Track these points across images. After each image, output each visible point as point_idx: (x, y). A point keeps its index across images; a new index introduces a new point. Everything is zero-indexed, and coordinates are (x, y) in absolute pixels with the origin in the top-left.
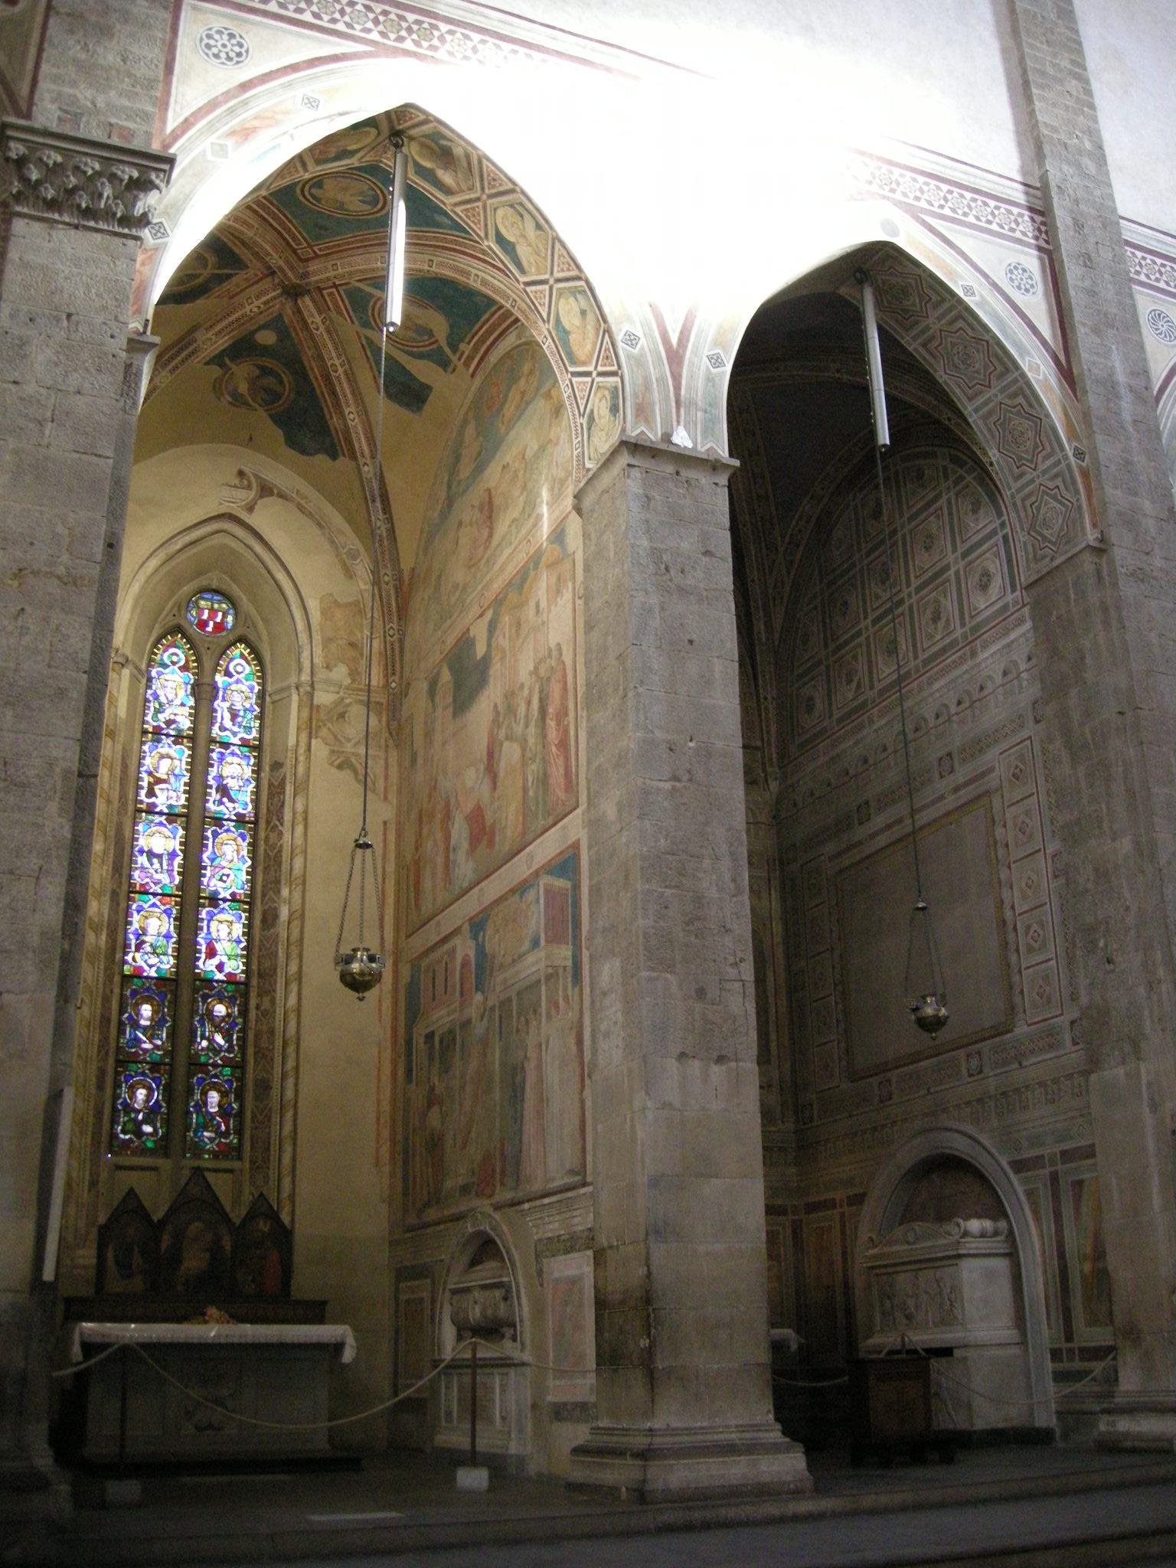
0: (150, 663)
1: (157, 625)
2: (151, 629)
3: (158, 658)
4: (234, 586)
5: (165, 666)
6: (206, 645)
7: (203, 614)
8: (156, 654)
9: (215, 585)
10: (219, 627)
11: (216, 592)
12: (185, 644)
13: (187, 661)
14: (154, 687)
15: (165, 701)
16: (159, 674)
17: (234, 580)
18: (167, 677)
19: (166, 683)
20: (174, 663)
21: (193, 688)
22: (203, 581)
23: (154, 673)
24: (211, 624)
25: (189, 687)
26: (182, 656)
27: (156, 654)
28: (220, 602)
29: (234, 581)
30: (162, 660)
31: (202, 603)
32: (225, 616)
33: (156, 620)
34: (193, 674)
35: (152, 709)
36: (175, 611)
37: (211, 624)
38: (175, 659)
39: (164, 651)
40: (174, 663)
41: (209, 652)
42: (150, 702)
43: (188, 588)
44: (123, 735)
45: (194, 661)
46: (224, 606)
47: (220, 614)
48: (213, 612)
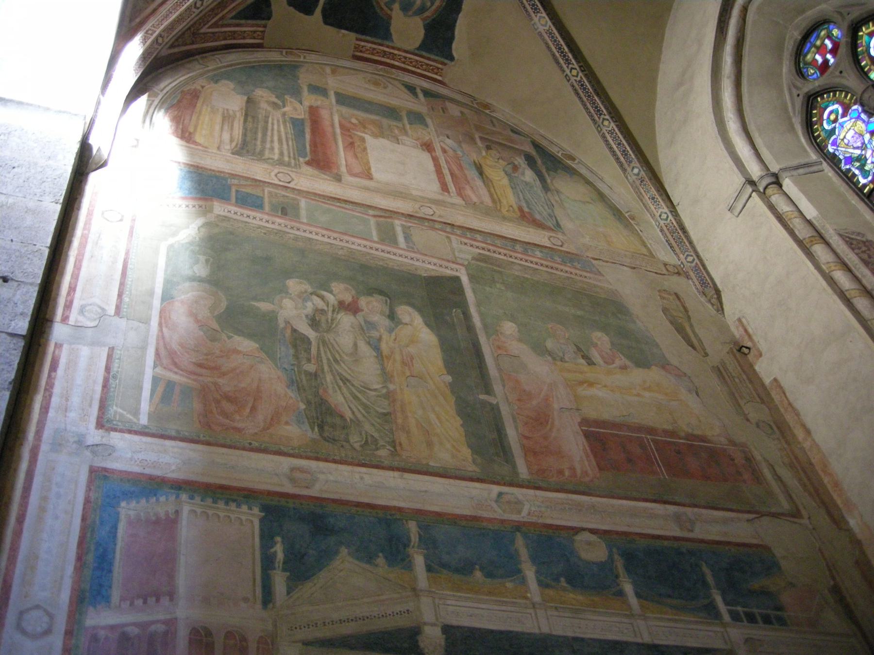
0: (820, 148)
1: (794, 120)
2: (792, 128)
3: (823, 134)
4: (809, 13)
5: (833, 131)
6: (837, 73)
7: (817, 61)
8: (819, 136)
9: (797, 35)
10: (834, 52)
11: (806, 36)
12: (828, 97)
13: (842, 104)
14: (841, 157)
15: (858, 152)
16: (834, 143)
17: (801, 11)
18: (842, 137)
19: (846, 141)
20: (835, 121)
21: (864, 111)
22: (789, 46)
23: (831, 149)
24: (829, 56)
25: (863, 116)
26: (836, 106)
27: (819, 136)
28: (818, 37)
29: (803, 11)
30: (826, 131)
31: (809, 57)
32: (829, 37)
33: (790, 118)
34: (855, 104)
35: (857, 172)
36: (795, 92)
37: (829, 56)
38: (832, 117)
39: (822, 125)
40: (835, 121)
41: (844, 74)
42: (849, 170)
43: (787, 67)
44: (828, 226)
45: (846, 96)
46: (823, 33)
47: (828, 42)
48: (821, 50)
